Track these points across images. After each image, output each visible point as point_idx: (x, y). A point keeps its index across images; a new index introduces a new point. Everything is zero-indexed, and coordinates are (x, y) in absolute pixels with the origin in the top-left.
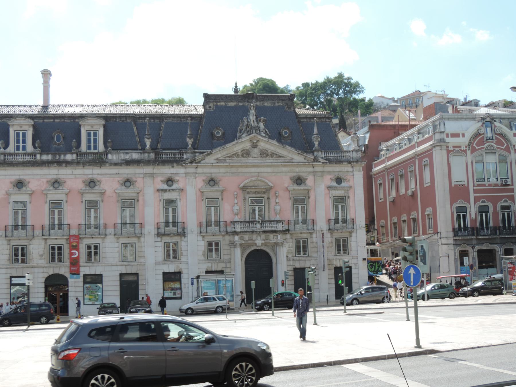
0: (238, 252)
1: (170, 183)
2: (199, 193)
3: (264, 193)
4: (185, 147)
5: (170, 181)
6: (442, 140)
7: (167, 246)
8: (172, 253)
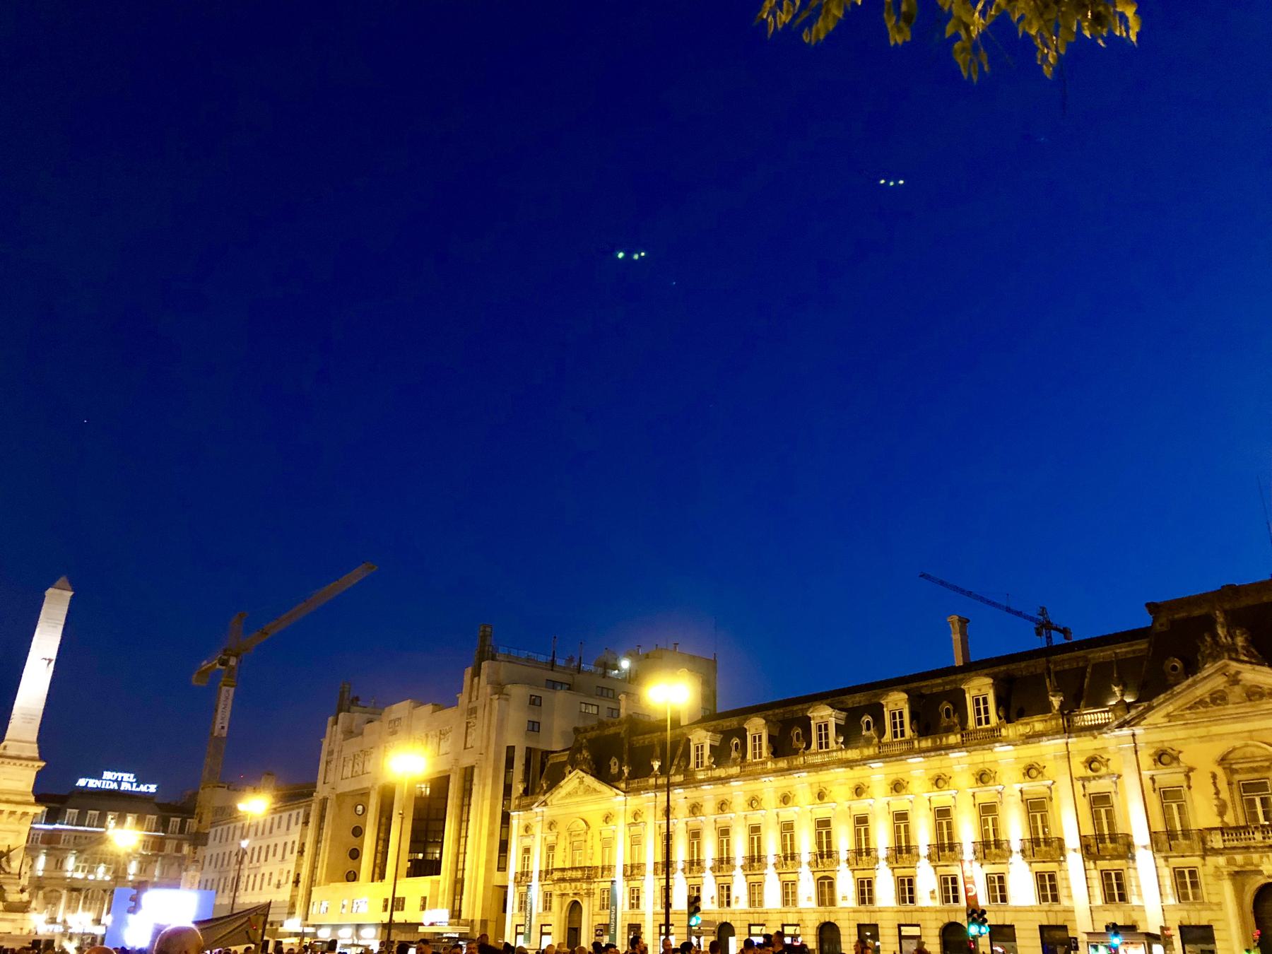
0: (1227, 888)
7: (1106, 875)
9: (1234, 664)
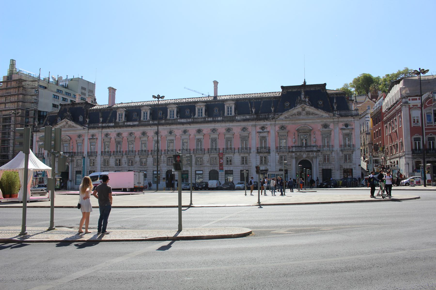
0: (294, 161)
1: (263, 129)
2: (277, 133)
3: (308, 132)
4: (270, 112)
5: (263, 128)
6: (406, 102)
7: (261, 158)
9: (305, 105)
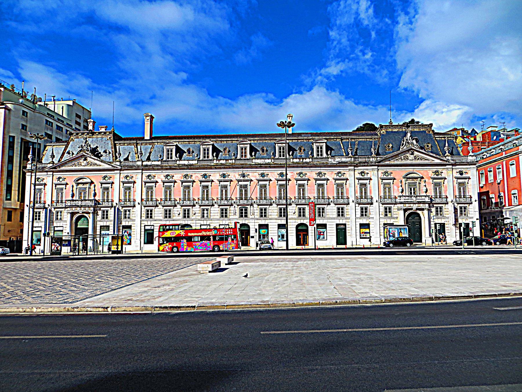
8: (364, 212)
